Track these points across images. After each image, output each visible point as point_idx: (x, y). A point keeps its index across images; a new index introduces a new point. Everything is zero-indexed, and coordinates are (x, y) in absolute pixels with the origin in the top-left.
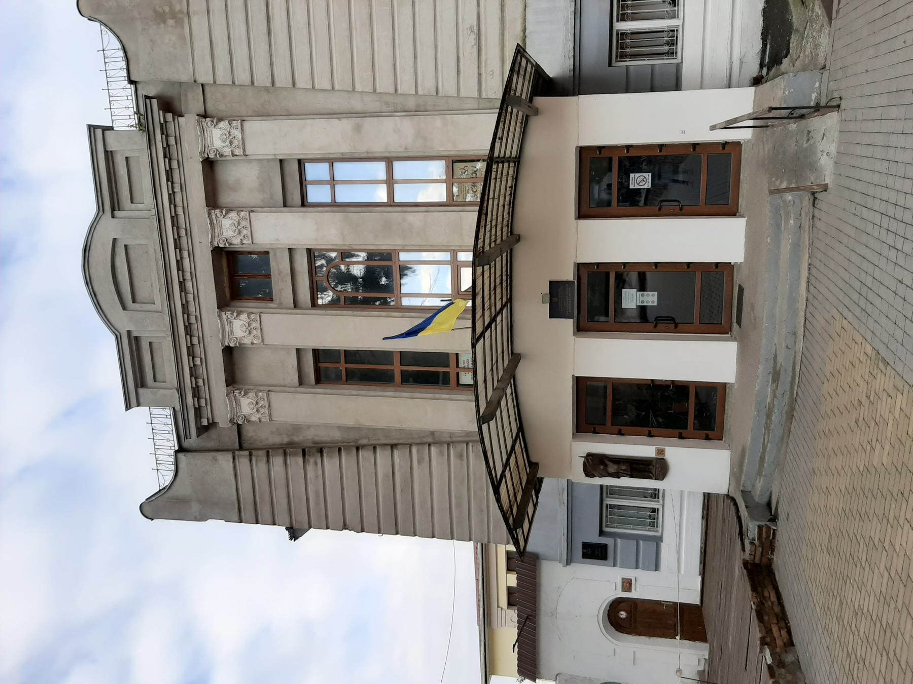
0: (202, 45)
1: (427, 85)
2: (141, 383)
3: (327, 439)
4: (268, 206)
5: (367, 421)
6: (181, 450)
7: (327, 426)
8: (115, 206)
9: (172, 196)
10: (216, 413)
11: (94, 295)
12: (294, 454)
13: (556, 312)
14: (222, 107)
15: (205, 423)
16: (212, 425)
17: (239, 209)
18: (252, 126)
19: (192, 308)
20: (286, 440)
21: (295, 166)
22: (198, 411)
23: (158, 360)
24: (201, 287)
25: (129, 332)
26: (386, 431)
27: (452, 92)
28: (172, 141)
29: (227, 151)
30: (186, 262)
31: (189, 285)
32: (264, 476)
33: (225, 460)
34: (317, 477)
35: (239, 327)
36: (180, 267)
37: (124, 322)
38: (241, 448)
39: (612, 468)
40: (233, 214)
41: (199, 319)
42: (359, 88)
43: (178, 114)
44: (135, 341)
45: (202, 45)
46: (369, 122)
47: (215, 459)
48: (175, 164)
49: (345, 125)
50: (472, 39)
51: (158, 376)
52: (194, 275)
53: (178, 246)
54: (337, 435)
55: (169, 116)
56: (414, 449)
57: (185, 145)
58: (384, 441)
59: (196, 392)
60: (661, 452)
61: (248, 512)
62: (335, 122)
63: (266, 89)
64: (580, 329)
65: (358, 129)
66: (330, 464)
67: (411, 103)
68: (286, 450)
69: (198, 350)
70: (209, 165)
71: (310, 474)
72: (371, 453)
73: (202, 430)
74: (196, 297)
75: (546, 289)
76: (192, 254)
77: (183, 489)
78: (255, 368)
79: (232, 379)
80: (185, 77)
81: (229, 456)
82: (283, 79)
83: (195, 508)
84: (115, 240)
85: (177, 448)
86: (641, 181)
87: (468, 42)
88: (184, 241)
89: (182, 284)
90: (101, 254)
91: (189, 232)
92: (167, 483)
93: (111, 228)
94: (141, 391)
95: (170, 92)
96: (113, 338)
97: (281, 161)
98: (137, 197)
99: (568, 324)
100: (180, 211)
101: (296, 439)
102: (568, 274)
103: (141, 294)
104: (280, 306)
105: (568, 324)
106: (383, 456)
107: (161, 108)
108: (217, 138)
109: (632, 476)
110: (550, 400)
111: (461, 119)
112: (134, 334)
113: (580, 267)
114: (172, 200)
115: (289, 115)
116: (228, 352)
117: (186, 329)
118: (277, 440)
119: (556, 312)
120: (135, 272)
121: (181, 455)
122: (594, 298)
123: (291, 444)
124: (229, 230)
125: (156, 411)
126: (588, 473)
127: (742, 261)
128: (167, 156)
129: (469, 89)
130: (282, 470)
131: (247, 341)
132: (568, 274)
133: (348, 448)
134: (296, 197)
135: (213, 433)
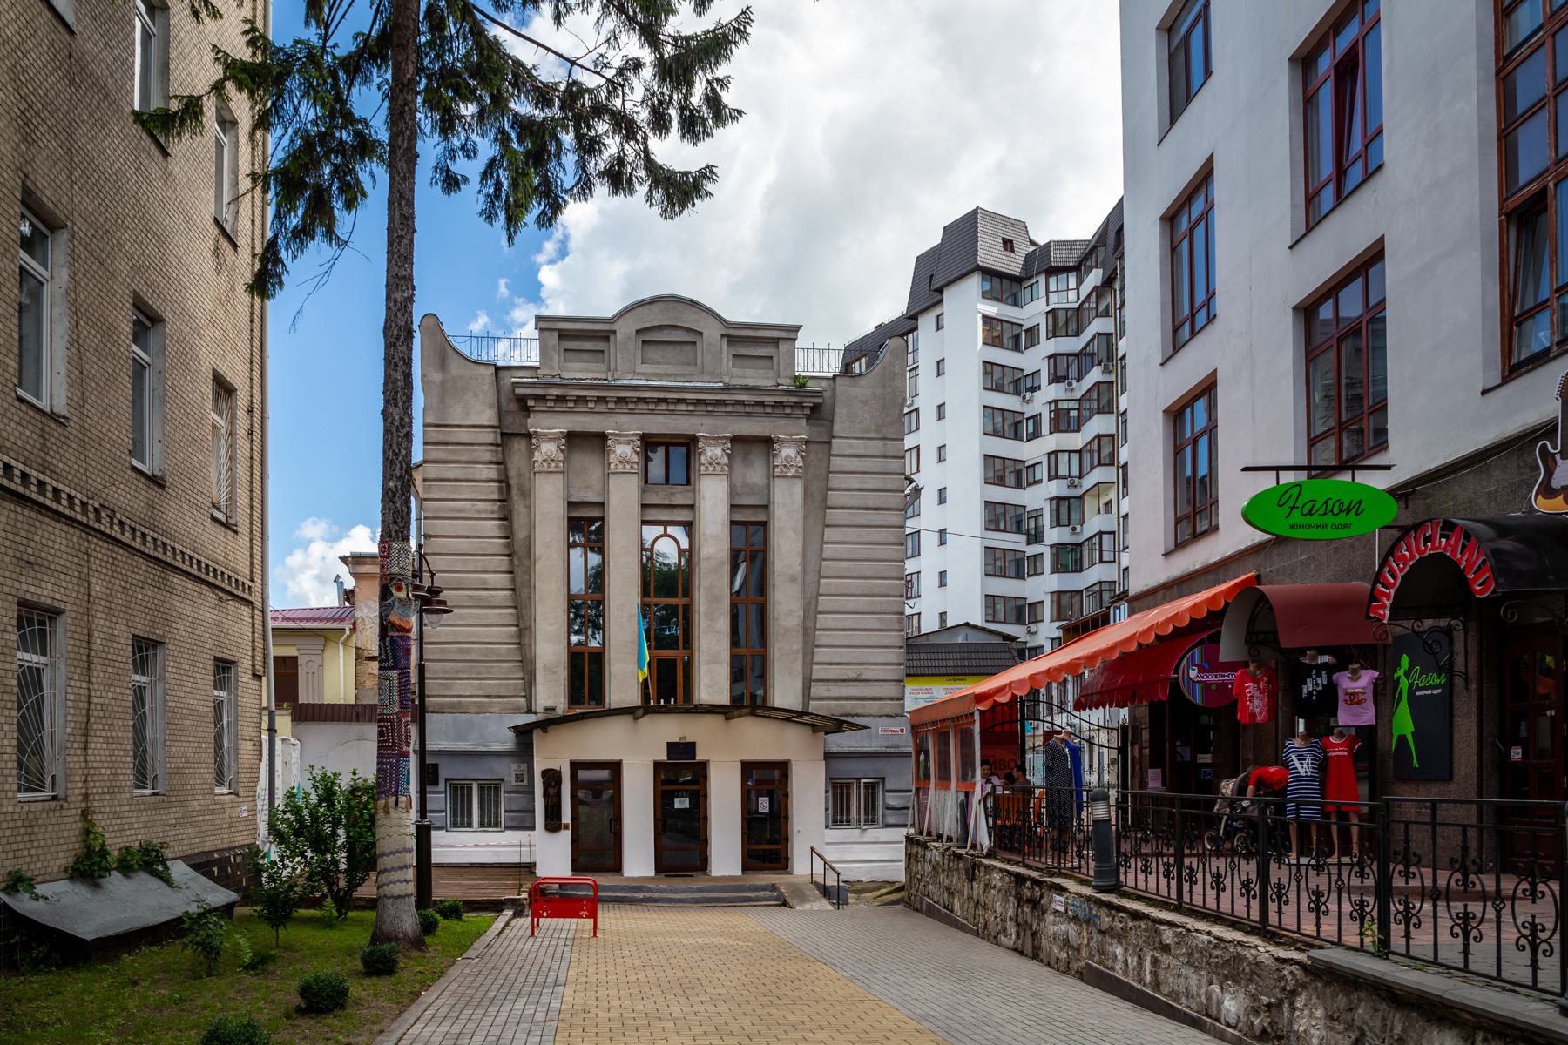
0: (859, 447)
1: (823, 638)
2: (563, 335)
3: (516, 525)
4: (732, 492)
5: (539, 567)
6: (497, 369)
7: (531, 526)
8: (731, 340)
9: (742, 403)
10: (540, 416)
11: (652, 302)
12: (500, 489)
13: (671, 747)
14: (812, 457)
15: (531, 403)
16: (526, 410)
17: (730, 465)
18: (798, 488)
19: (642, 406)
20: (513, 482)
21: (762, 518)
22: (543, 398)
23: (585, 356)
24: (661, 419)
25: (614, 332)
26: (530, 586)
27: (816, 659)
28: (788, 411)
29: (778, 462)
30: (683, 407)
31: (663, 407)
32: (475, 457)
33: (487, 416)
34: (479, 512)
35: (623, 451)
36: (680, 401)
37: (624, 330)
38: (502, 434)
39: (552, 791)
40: (726, 460)
41: (631, 412)
42: (823, 581)
43: (808, 417)
44: (606, 336)
45: (859, 447)
46: (796, 590)
47: (491, 406)
48: (769, 410)
49: (797, 569)
50: (853, 675)
51: (569, 354)
52: (672, 412)
53: (699, 402)
54: (520, 534)
55: (807, 411)
56: (512, 611)
57: (783, 422)
58: (518, 580)
59: (561, 399)
60: (566, 827)
61: (436, 435)
62: (799, 560)
63: (825, 499)
64: (658, 765)
65: (793, 579)
66: (492, 527)
67: (810, 624)
68: (504, 482)
69: (601, 407)
70: (767, 442)
71: (481, 505)
72: (505, 568)
73: (522, 401)
74: (652, 412)
75: (689, 740)
76: (690, 413)
77: (456, 367)
78: (586, 461)
79: (574, 440)
80: (837, 428)
81: (494, 423)
82: (834, 516)
83: (436, 376)
84: (701, 334)
85: (499, 364)
86: (764, 805)
87: (850, 672)
88: (702, 408)
89: (664, 400)
90: (690, 319)
91: (710, 414)
92: (456, 346)
93: (712, 333)
94: (556, 334)
95: (826, 410)
96: (609, 315)
97: (767, 507)
98: (739, 362)
99: (663, 757)
100: (729, 409)
101: (514, 492)
102: (700, 756)
103: (653, 353)
104: (643, 491)
105: (663, 757)
106: (502, 579)
107: (812, 406)
108: (787, 452)
109: (546, 807)
110: (599, 741)
111: (798, 666)
112: (612, 338)
113: (704, 765)
114: (738, 402)
115: (805, 517)
116: (602, 438)
117: (626, 401)
118: (512, 473)
119: (671, 747)
120: (670, 348)
121: (492, 370)
122: (681, 775)
123: (509, 487)
124: (713, 453)
125: (535, 346)
126: (545, 773)
127: (714, 874)
128: (777, 405)
129: (819, 671)
130: (484, 477)
131: (612, 457)
132: (700, 757)
133: (509, 546)
134: (739, 517)
135: (513, 406)
